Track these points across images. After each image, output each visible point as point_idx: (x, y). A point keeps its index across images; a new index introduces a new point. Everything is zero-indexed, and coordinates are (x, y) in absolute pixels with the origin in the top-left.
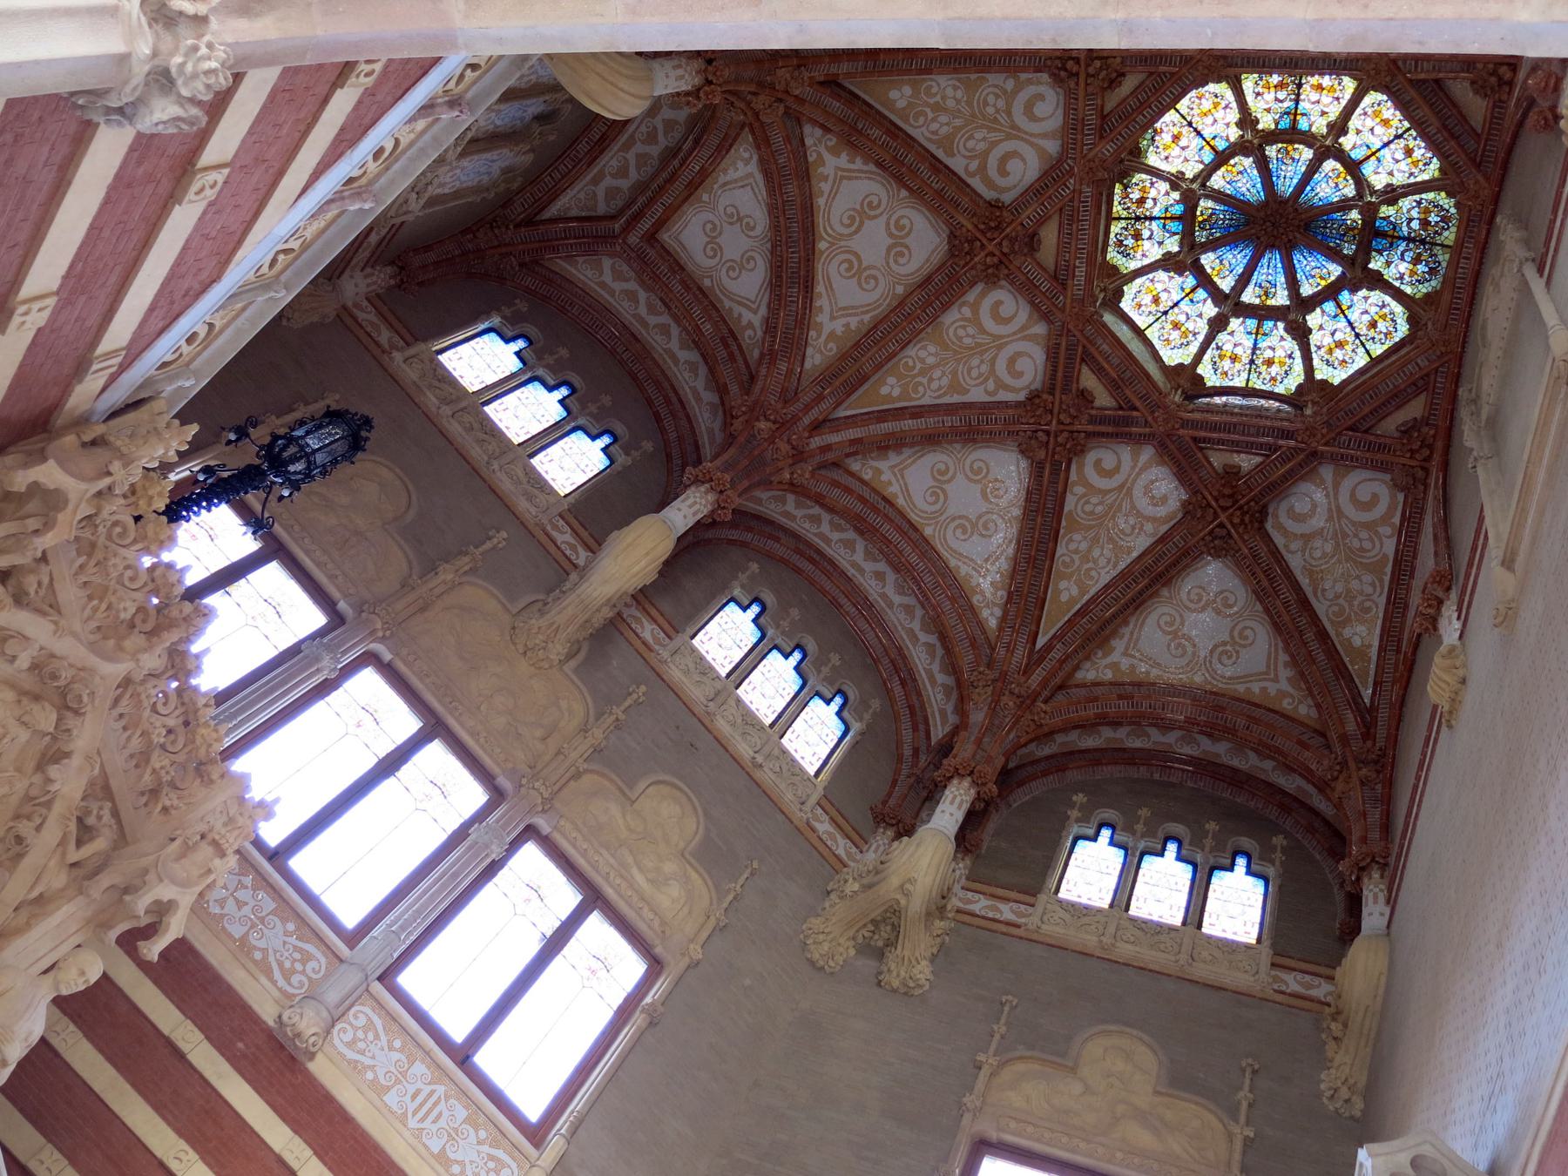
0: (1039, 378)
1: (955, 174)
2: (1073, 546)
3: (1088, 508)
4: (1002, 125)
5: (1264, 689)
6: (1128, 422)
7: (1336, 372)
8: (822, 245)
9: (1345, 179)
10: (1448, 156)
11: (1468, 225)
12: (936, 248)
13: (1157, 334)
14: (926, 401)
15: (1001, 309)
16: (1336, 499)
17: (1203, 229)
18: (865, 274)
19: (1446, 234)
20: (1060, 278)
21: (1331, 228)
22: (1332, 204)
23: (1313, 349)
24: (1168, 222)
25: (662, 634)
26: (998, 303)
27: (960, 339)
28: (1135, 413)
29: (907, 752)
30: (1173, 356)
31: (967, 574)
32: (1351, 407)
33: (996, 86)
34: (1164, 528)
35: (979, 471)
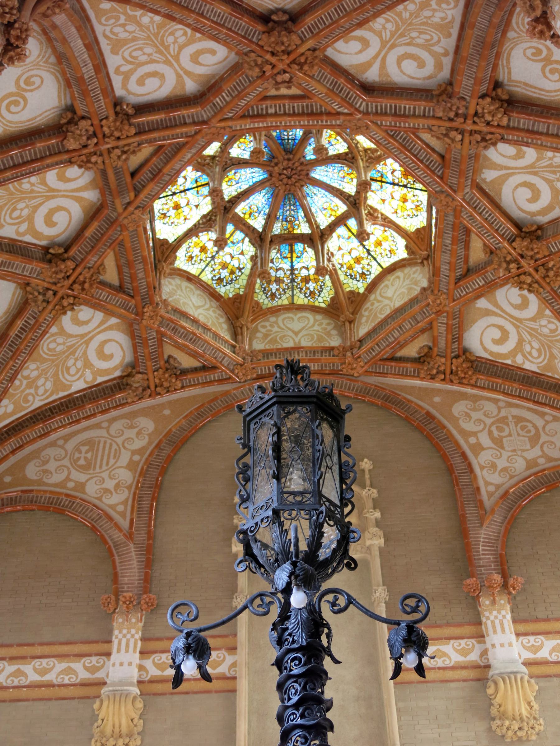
4: (396, 40)
9: (331, 215)
10: (378, 345)
11: (330, 363)
15: (208, 56)
16: (99, 333)
19: (302, 296)
21: (290, 210)
22: (311, 211)
26: (213, 52)
28: (132, 194)
32: (180, 329)
33: (439, 41)
34: (28, 238)
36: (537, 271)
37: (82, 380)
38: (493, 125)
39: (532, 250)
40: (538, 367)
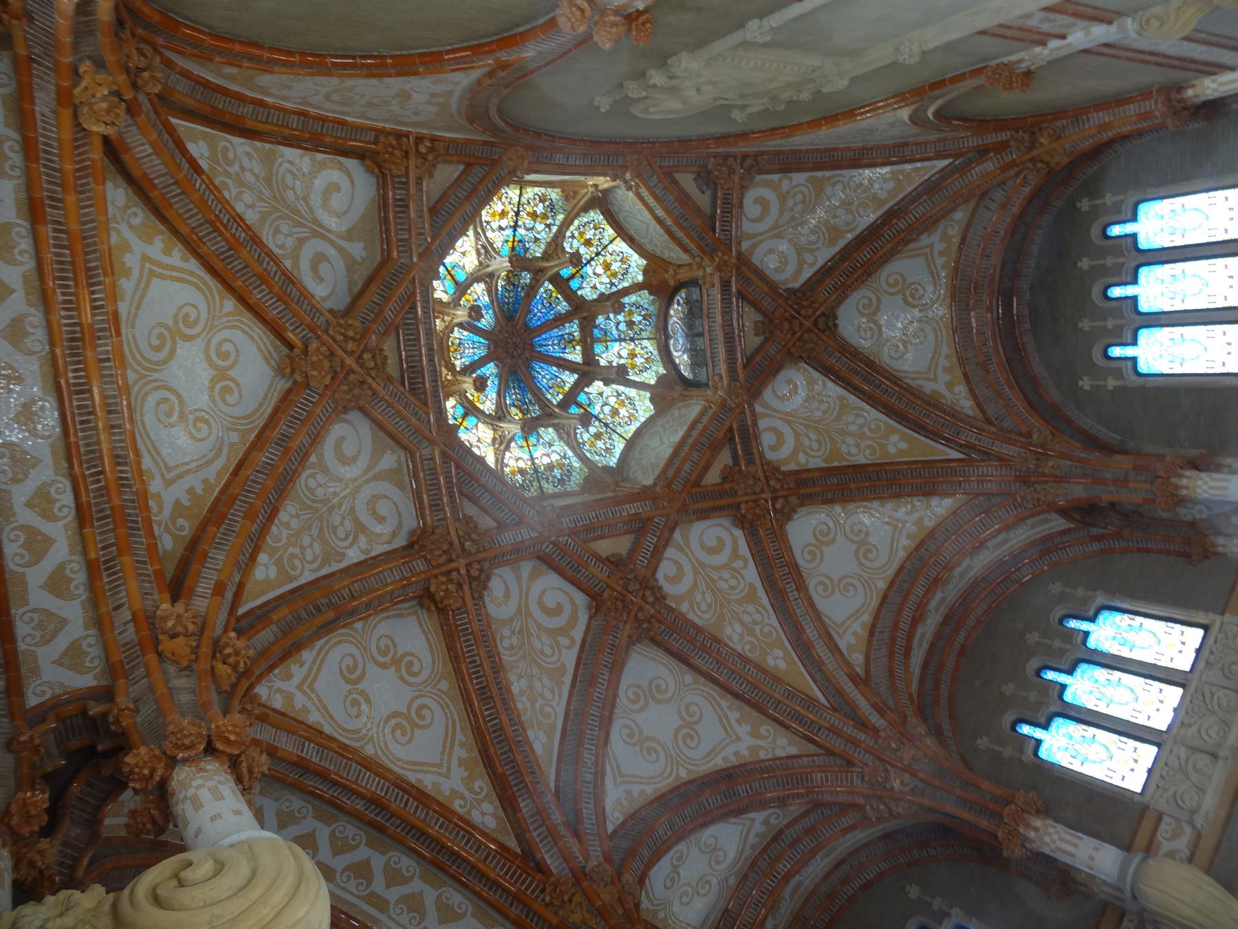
0: (717, 521)
1: (579, 659)
2: (854, 450)
3: (815, 446)
5: (941, 254)
6: (744, 429)
7: (633, 264)
8: (684, 774)
11: (542, 163)
12: (639, 653)
13: (627, 428)
14: (774, 621)
15: (671, 574)
16: (761, 234)
17: (528, 410)
18: (688, 718)
20: (639, 526)
22: (492, 301)
23: (614, 289)
24: (530, 443)
25: (1163, 826)
27: (709, 606)
29: (1096, 546)
30: (644, 408)
31: (908, 537)
34: (816, 375)
35: (812, 553)
36: (343, 365)
37: (793, 185)
38: (442, 574)
39: (354, 396)
40: (282, 156)
